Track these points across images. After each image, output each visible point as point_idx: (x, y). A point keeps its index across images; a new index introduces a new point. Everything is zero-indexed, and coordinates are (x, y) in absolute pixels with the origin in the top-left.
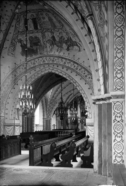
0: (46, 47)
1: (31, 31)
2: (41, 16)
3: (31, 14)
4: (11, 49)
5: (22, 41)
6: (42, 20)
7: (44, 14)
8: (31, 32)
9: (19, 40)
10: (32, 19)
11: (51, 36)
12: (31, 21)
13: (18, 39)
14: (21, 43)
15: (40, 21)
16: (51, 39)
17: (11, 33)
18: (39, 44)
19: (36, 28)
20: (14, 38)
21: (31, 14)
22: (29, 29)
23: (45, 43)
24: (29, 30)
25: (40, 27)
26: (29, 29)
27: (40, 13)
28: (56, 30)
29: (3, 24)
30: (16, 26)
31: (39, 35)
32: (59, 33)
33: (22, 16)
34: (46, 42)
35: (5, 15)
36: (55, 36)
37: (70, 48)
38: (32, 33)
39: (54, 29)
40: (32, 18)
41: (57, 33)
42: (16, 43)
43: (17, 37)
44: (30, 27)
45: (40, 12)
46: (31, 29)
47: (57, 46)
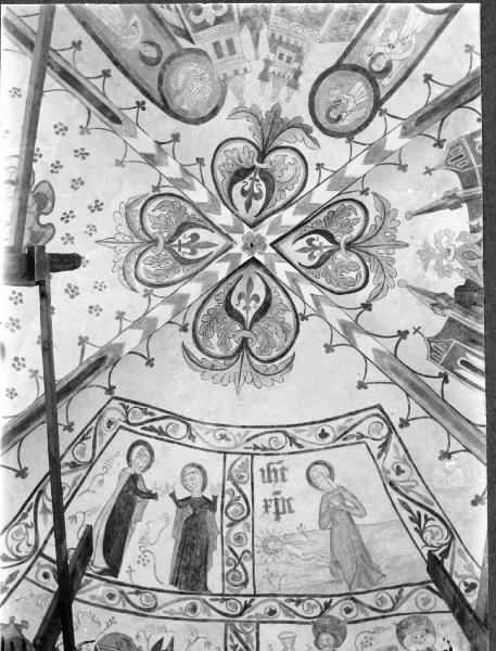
1: (139, 590)
2: (263, 491)
6: (264, 523)
7: (296, 466)
10: (180, 504)
12: (167, 519)
15: (239, 528)
22: (130, 571)
24: (123, 576)
25: (224, 576)
26: (130, 571)
27: (261, 462)
28: (368, 599)
32: (400, 631)
33: (125, 439)
38: (143, 612)
39: (350, 596)
40: (180, 496)
41: (370, 625)
44: (142, 561)
45: (268, 452)
46: (144, 578)
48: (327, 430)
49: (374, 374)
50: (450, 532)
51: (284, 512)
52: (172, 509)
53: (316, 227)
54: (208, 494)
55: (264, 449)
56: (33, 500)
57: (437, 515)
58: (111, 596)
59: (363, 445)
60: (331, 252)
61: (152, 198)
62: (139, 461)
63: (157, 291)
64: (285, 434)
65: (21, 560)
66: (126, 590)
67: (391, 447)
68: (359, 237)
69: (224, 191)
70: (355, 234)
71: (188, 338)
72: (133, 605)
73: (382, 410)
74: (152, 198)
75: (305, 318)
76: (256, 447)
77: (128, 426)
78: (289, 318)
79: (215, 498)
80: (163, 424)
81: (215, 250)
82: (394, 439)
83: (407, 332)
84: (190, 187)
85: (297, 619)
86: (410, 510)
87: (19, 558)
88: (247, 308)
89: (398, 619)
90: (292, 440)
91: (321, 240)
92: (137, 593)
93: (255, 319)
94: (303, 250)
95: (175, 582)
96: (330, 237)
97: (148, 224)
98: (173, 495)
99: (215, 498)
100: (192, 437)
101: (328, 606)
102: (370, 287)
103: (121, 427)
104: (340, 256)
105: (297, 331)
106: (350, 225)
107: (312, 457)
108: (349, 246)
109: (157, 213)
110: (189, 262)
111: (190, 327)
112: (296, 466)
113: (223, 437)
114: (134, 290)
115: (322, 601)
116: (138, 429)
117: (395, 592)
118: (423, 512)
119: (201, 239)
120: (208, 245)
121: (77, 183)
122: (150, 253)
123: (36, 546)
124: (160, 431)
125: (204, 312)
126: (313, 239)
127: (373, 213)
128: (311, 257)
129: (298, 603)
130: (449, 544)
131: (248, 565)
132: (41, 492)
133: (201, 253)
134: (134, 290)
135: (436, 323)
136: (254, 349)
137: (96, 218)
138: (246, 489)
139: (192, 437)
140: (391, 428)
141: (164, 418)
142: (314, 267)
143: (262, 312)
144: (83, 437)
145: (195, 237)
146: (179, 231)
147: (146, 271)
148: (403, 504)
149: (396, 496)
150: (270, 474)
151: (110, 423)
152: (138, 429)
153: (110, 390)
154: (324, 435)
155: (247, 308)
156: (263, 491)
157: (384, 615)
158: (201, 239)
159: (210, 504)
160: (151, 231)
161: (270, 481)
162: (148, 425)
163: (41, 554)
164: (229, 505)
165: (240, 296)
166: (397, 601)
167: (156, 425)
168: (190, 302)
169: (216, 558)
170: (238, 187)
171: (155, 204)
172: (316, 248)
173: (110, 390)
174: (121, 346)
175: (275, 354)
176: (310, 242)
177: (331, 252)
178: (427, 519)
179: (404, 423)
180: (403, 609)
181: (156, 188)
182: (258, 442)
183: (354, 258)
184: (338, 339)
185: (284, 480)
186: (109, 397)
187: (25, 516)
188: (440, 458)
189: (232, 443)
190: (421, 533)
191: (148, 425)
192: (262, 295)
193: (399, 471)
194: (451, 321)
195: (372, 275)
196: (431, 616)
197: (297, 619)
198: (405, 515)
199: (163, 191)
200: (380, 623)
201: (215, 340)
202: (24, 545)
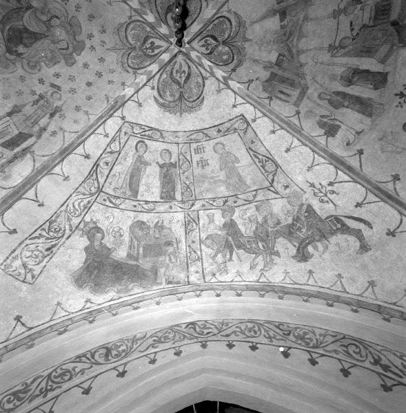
0: (200, 259)
1: (147, 202)
3: (165, 146)
4: (32, 247)
5: (98, 229)
8: (145, 206)
9: (86, 224)
10: (161, 167)
11: (223, 221)
13: (88, 219)
14: (91, 238)
16: (219, 233)
17: (66, 178)
18: (170, 249)
19: (168, 196)
20: (71, 206)
21: (165, 146)
23: (196, 246)
24: (139, 198)
27: (194, 146)
29: (54, 133)
30: (96, 165)
31: (175, 219)
32: (257, 208)
33: (133, 142)
34: (201, 241)
35: (78, 109)
36: (239, 222)
37: (310, 249)
38: (149, 211)
40: (161, 162)
42: (68, 232)
43: (88, 208)
44: (148, 190)
47: (249, 251)
48: (221, 129)
49: (239, 100)
50: (276, 165)
51: (205, 166)
52: (158, 169)
53: (208, 34)
54: (172, 161)
55: (195, 140)
56: (95, 168)
57: (270, 159)
58: (135, 206)
59: (237, 134)
60: (216, 46)
61: (129, 24)
62: (141, 150)
63: (138, 71)
64: (203, 133)
65: (92, 195)
66: (141, 203)
67: (248, 132)
68: (228, 38)
69: (163, 17)
70: (226, 36)
71: (155, 93)
72: (145, 209)
73: (244, 116)
74: (129, 24)
75: (207, 79)
76: (191, 140)
77: (134, 135)
78: (200, 80)
79: (176, 162)
80: (150, 132)
81: (163, 49)
82: (250, 129)
83: (253, 80)
84: (146, 14)
85: (213, 208)
86: (259, 159)
87: (91, 194)
88: (180, 77)
89: (256, 204)
90: (207, 135)
91: (211, 41)
92: (146, 204)
93: (185, 82)
94: (202, 46)
95: (162, 198)
96: (215, 38)
97: (130, 39)
98: (157, 163)
99: (176, 162)
100: (163, 138)
101: (226, 201)
102: (235, 61)
103: (131, 135)
104: (220, 48)
105: (204, 86)
106: (223, 31)
107: (216, 141)
108: (224, 43)
109: (133, 32)
110: (151, 56)
111: (156, 88)
112: (209, 146)
113: (177, 137)
114: (128, 72)
115: (224, 199)
116: (139, 135)
117: (254, 193)
118: (264, 158)
119: (156, 44)
120: (159, 47)
121: (91, 17)
122: (133, 54)
123: (99, 188)
124: (148, 136)
125: (162, 80)
126: (207, 40)
127: (234, 23)
128: (207, 49)
129: (214, 201)
130: (276, 170)
131: (192, 188)
132: (98, 165)
133: (156, 51)
134: (128, 72)
135: (265, 75)
136: (186, 97)
137: (106, 38)
138: (189, 158)
139: (163, 138)
140: (248, 124)
141: (150, 130)
142: (209, 54)
143: (188, 78)
144: (113, 140)
145: (152, 43)
146: (145, 42)
147: (132, 63)
148: (255, 156)
149: (252, 153)
150: (197, 151)
151: (126, 133)
152: (139, 135)
153: (123, 118)
154: (219, 131)
155: (180, 77)
156: (196, 158)
157: (250, 202)
158: (156, 44)
159: (173, 165)
160: (132, 42)
161: (198, 153)
162: (143, 134)
163: (101, 191)
164: (182, 164)
165: (177, 72)
166: (255, 196)
167: (147, 133)
168: (154, 73)
169: (179, 187)
170: (169, 16)
171: (132, 26)
172: (209, 44)
173: (123, 118)
174: (124, 96)
175: (195, 98)
176: (206, 41)
177: (216, 46)
178: (266, 161)
179: (254, 121)
180: (257, 199)
181: (130, 17)
182: (192, 137)
183: (227, 49)
184: (222, 86)
185: (204, 152)
186: (123, 121)
187: (92, 176)
188: (331, 48)
189: (181, 139)
190: (263, 167)
191: (143, 134)
192: (187, 71)
193: (253, 142)
194: (272, 72)
195: (235, 57)
196: (271, 201)
197: (213, 208)
198: (257, 160)
199: (133, 18)
200: (249, 206)
201: (168, 93)
202: (92, 189)
